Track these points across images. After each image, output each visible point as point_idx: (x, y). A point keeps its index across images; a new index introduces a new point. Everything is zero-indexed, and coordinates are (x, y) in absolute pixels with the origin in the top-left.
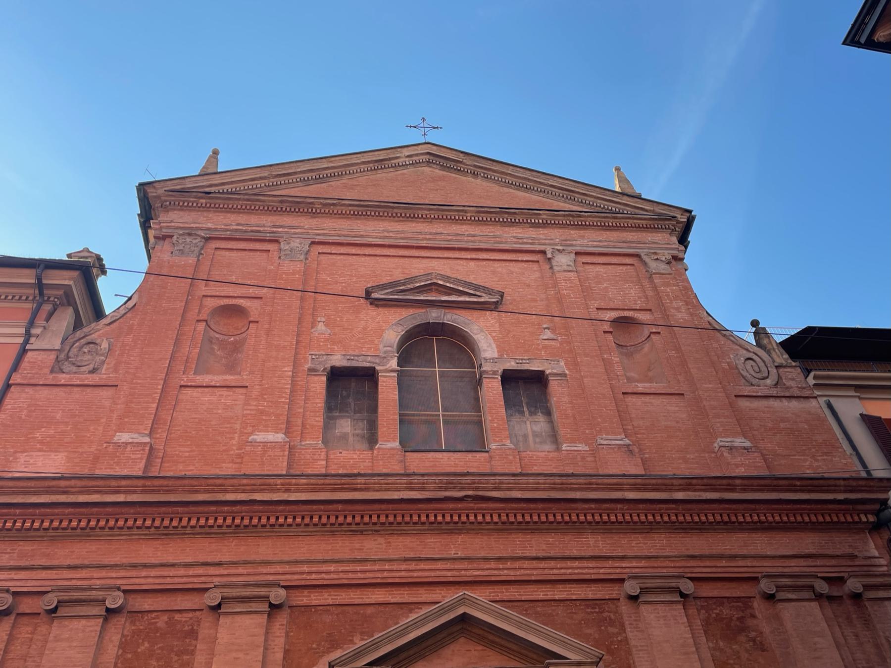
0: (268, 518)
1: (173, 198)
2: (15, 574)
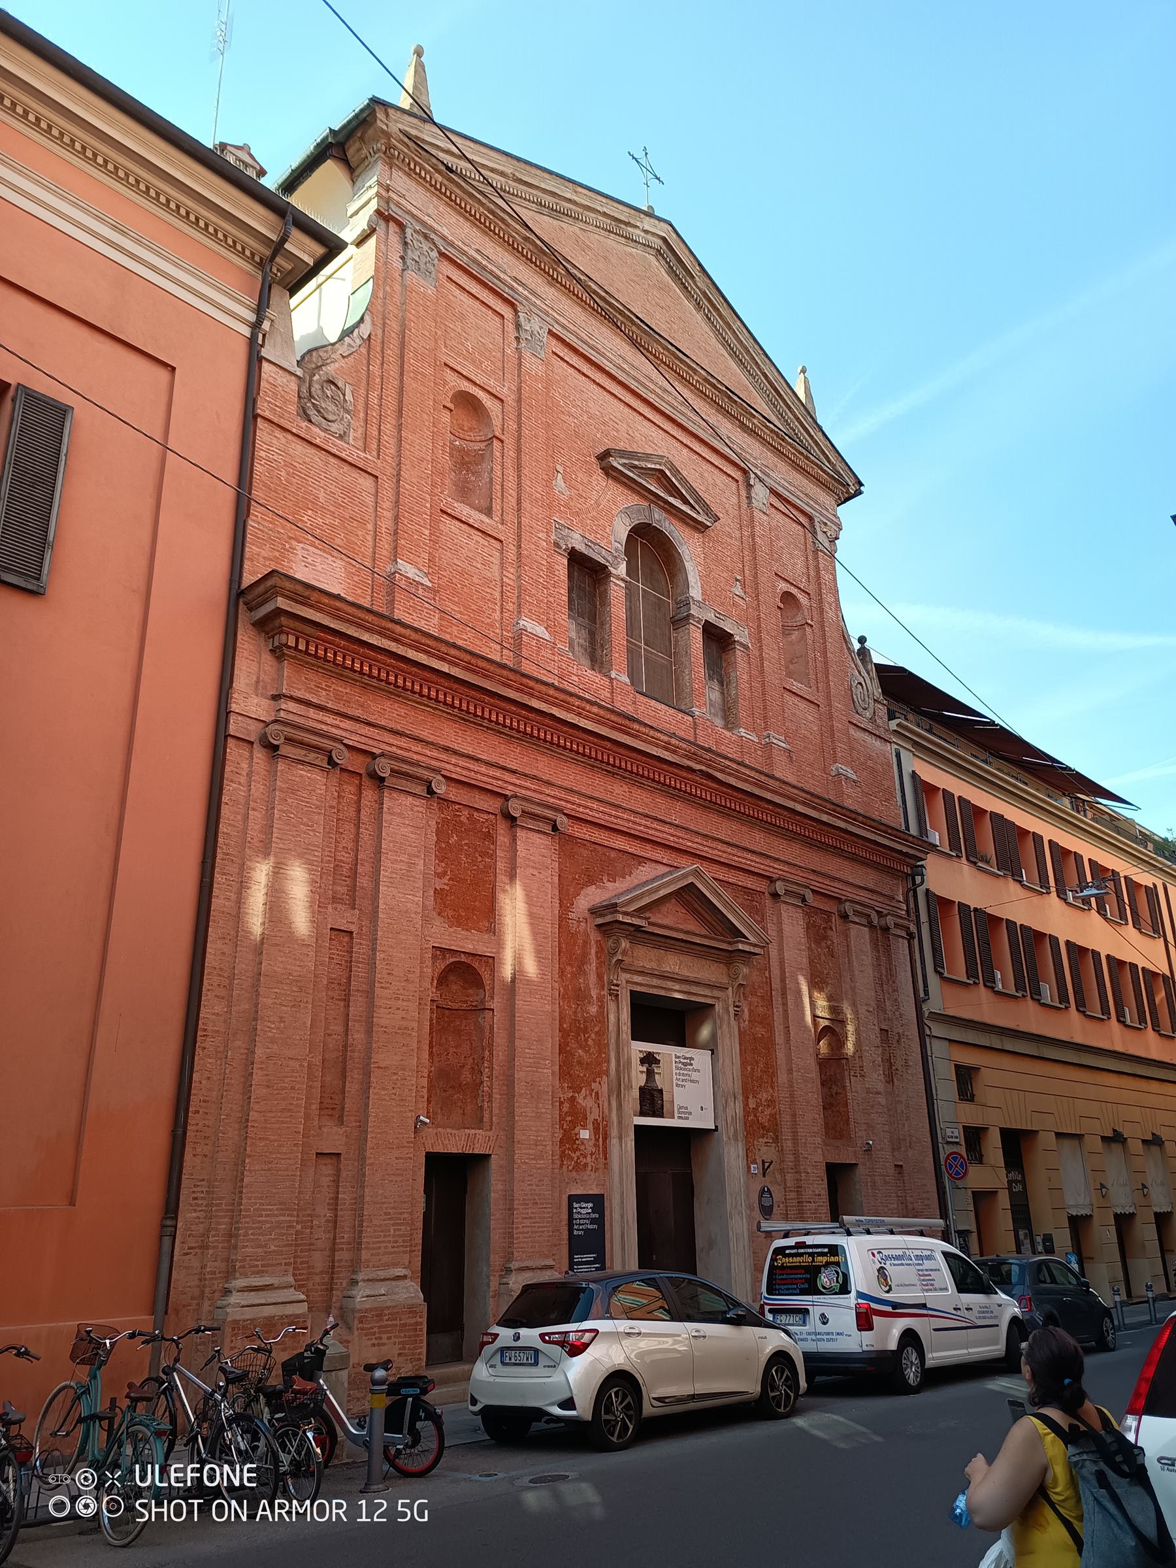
1: (406, 150)
2: (341, 721)
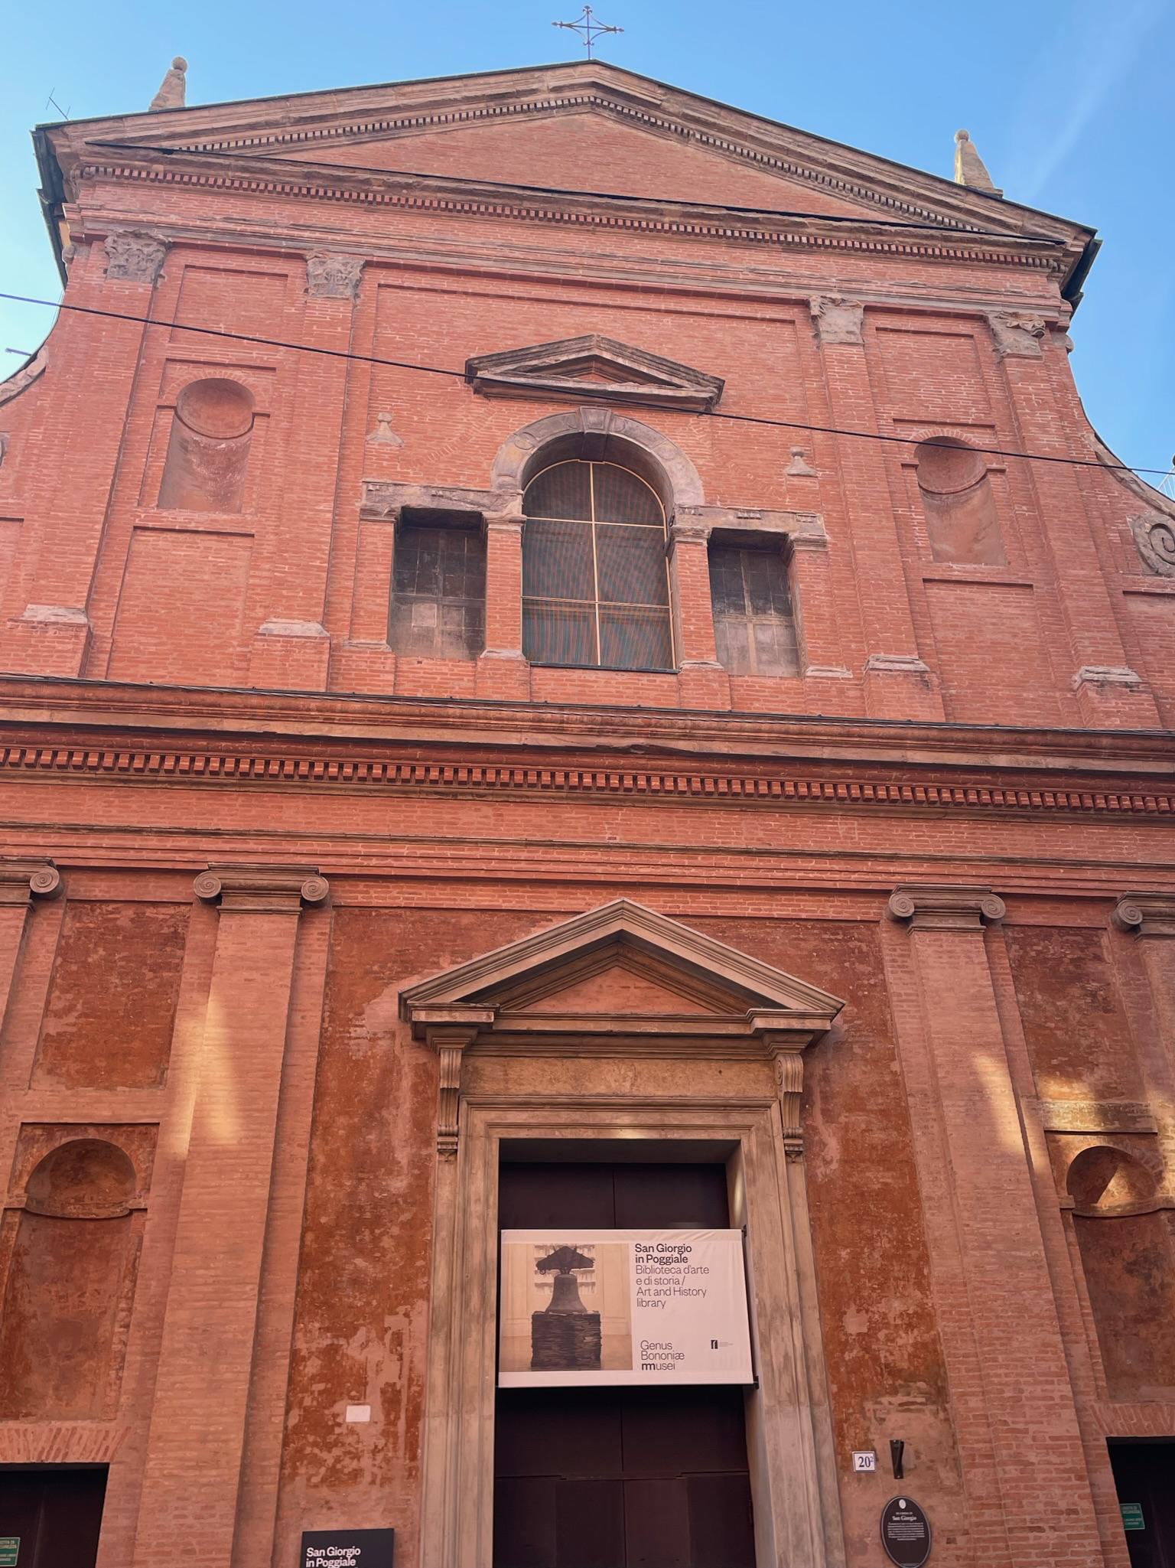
0: (297, 765)
